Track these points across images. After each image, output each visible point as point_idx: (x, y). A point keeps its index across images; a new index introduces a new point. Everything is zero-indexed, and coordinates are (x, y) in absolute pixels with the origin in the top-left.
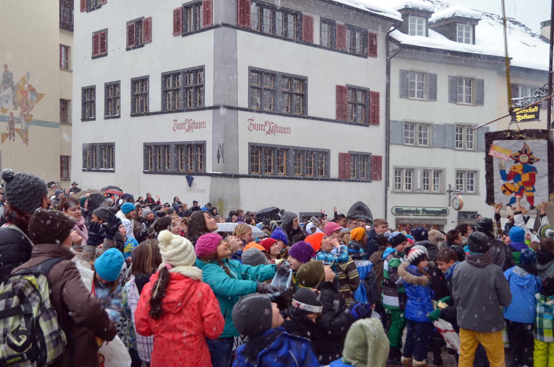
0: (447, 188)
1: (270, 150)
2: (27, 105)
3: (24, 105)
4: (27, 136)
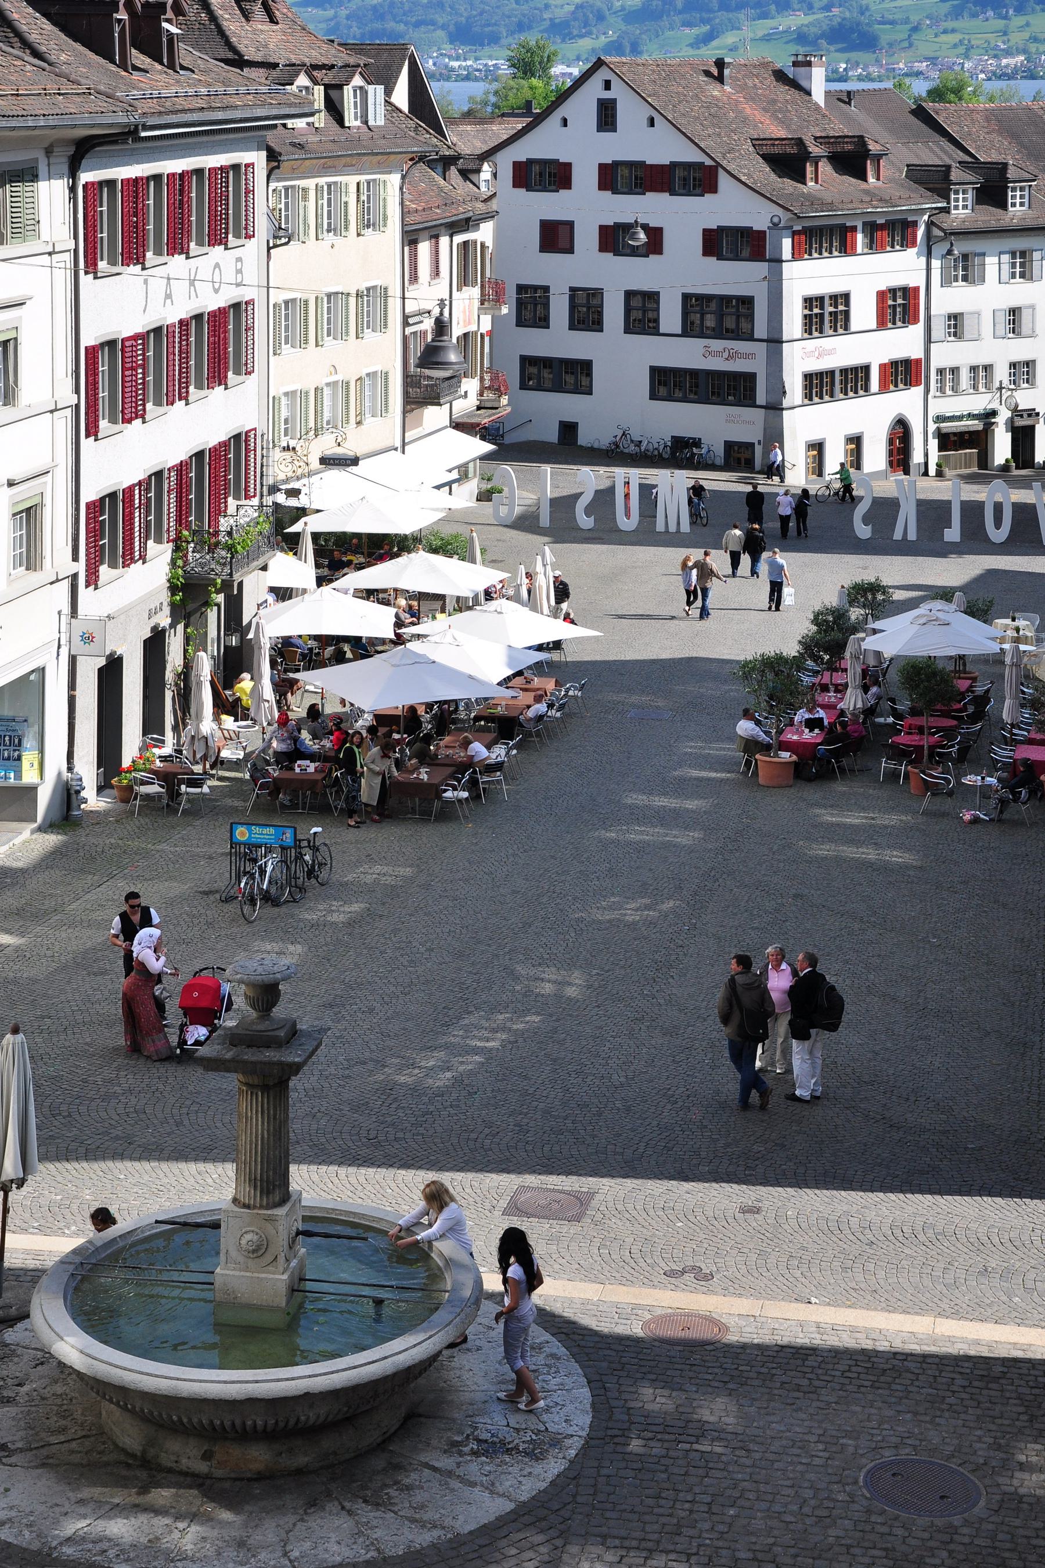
0: (997, 385)
1: (820, 375)
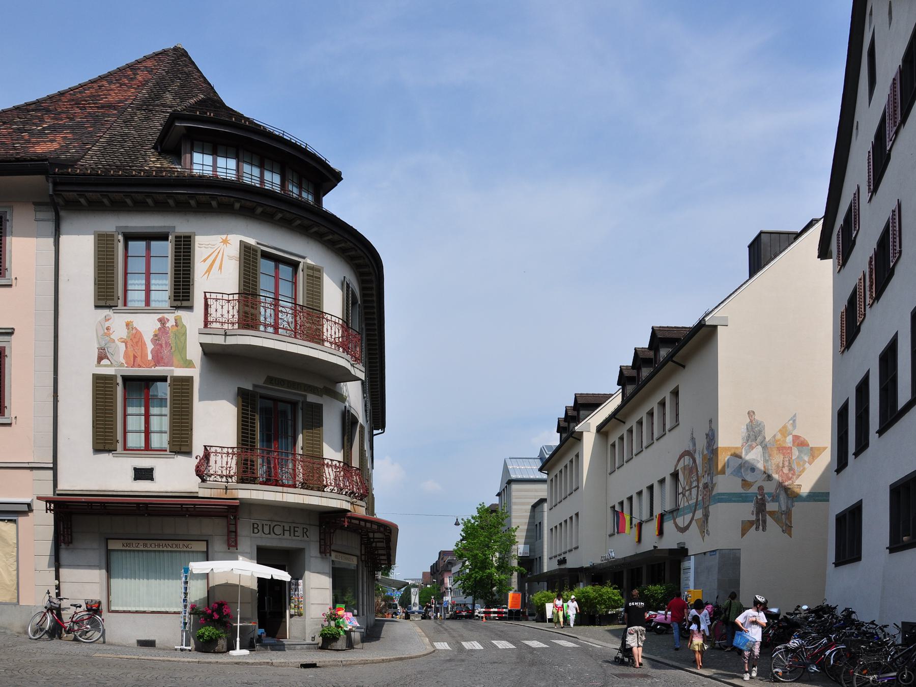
2: (791, 469)
3: (786, 470)
4: (791, 522)
